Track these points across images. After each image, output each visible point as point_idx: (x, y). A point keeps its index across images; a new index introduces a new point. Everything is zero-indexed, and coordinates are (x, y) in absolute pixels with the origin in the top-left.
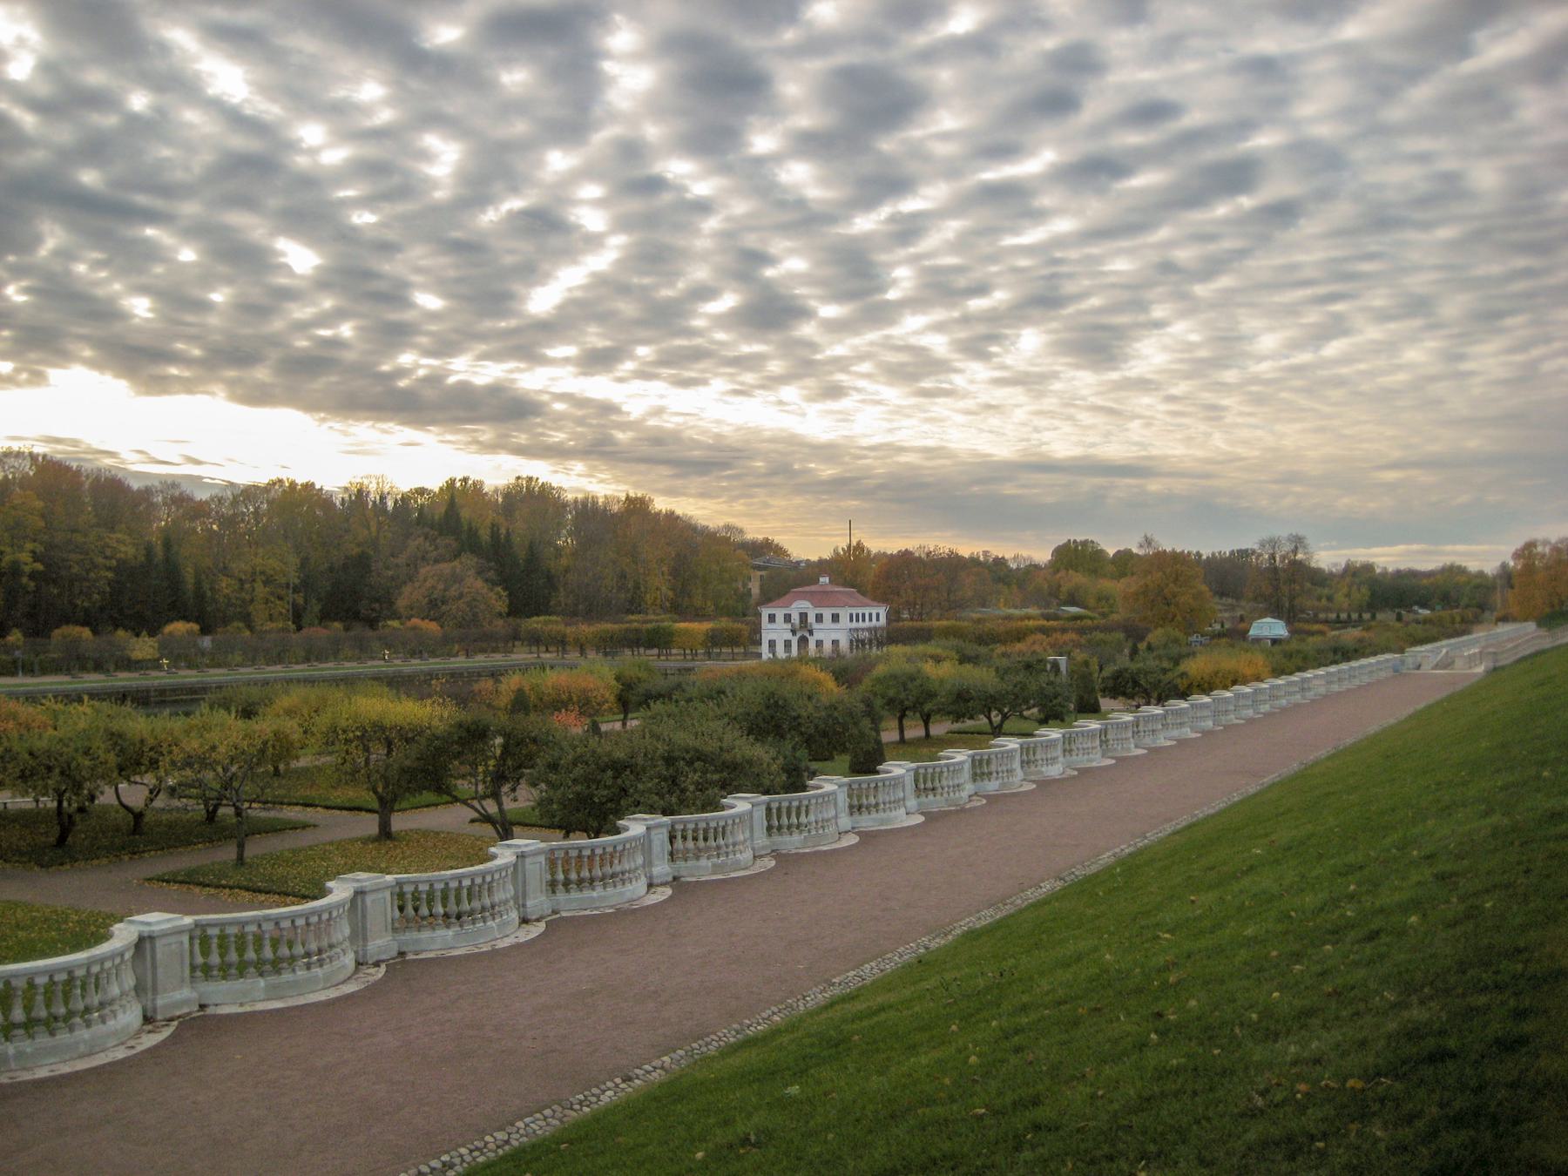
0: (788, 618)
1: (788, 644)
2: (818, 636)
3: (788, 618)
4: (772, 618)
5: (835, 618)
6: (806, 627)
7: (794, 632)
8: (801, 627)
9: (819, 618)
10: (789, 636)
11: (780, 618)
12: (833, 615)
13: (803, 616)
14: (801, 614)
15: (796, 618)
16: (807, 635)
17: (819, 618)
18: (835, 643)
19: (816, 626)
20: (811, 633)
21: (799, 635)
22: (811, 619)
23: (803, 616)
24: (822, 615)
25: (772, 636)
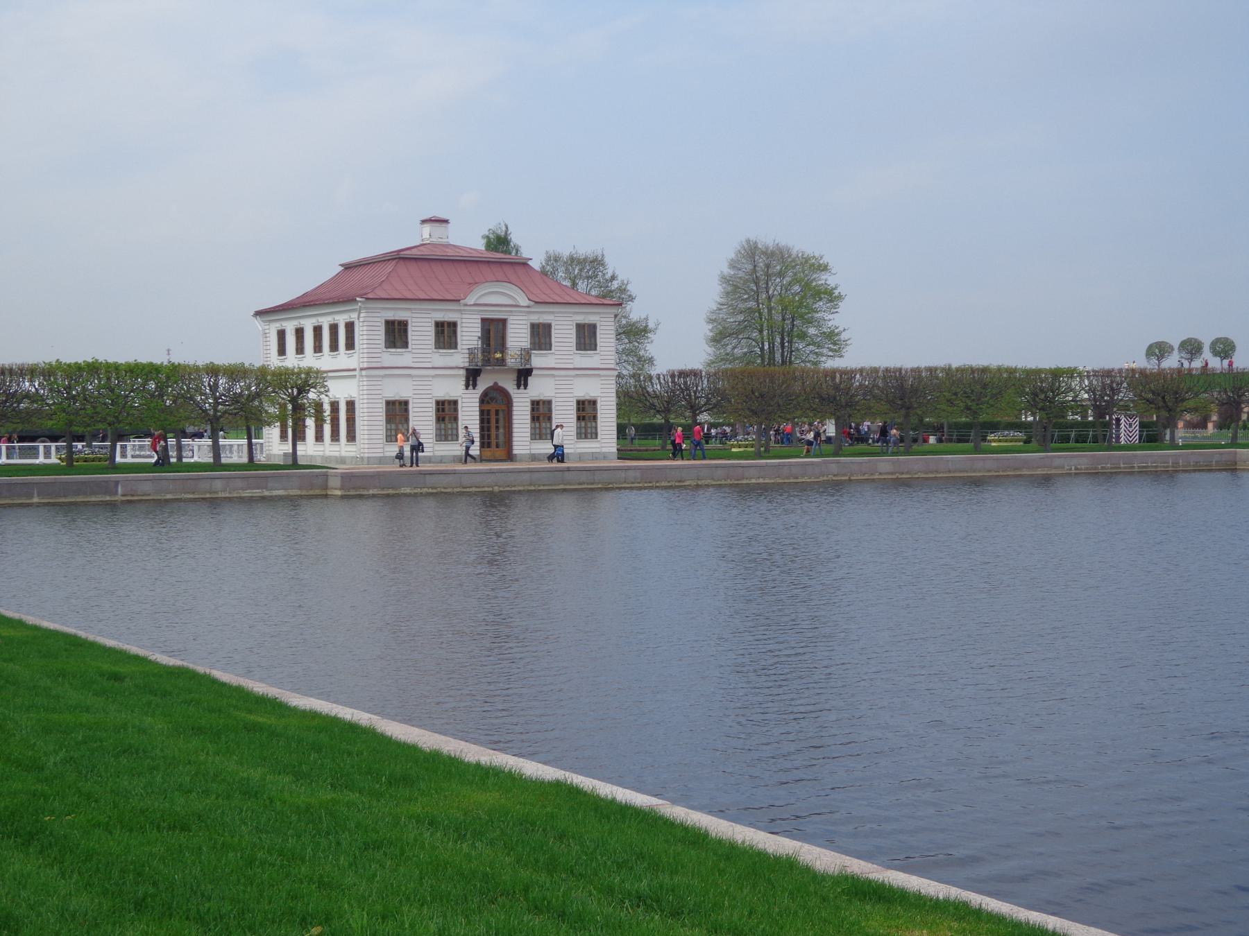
1: (446, 411)
2: (539, 388)
3: (446, 334)
4: (396, 334)
6: (502, 362)
7: (472, 376)
8: (487, 361)
9: (541, 336)
10: (454, 388)
12: (580, 328)
13: (493, 331)
15: (470, 335)
16: (509, 385)
17: (541, 336)
18: (586, 411)
20: (523, 376)
21: (484, 384)
22: (518, 337)
23: (493, 331)
24: (547, 328)
25: (398, 389)
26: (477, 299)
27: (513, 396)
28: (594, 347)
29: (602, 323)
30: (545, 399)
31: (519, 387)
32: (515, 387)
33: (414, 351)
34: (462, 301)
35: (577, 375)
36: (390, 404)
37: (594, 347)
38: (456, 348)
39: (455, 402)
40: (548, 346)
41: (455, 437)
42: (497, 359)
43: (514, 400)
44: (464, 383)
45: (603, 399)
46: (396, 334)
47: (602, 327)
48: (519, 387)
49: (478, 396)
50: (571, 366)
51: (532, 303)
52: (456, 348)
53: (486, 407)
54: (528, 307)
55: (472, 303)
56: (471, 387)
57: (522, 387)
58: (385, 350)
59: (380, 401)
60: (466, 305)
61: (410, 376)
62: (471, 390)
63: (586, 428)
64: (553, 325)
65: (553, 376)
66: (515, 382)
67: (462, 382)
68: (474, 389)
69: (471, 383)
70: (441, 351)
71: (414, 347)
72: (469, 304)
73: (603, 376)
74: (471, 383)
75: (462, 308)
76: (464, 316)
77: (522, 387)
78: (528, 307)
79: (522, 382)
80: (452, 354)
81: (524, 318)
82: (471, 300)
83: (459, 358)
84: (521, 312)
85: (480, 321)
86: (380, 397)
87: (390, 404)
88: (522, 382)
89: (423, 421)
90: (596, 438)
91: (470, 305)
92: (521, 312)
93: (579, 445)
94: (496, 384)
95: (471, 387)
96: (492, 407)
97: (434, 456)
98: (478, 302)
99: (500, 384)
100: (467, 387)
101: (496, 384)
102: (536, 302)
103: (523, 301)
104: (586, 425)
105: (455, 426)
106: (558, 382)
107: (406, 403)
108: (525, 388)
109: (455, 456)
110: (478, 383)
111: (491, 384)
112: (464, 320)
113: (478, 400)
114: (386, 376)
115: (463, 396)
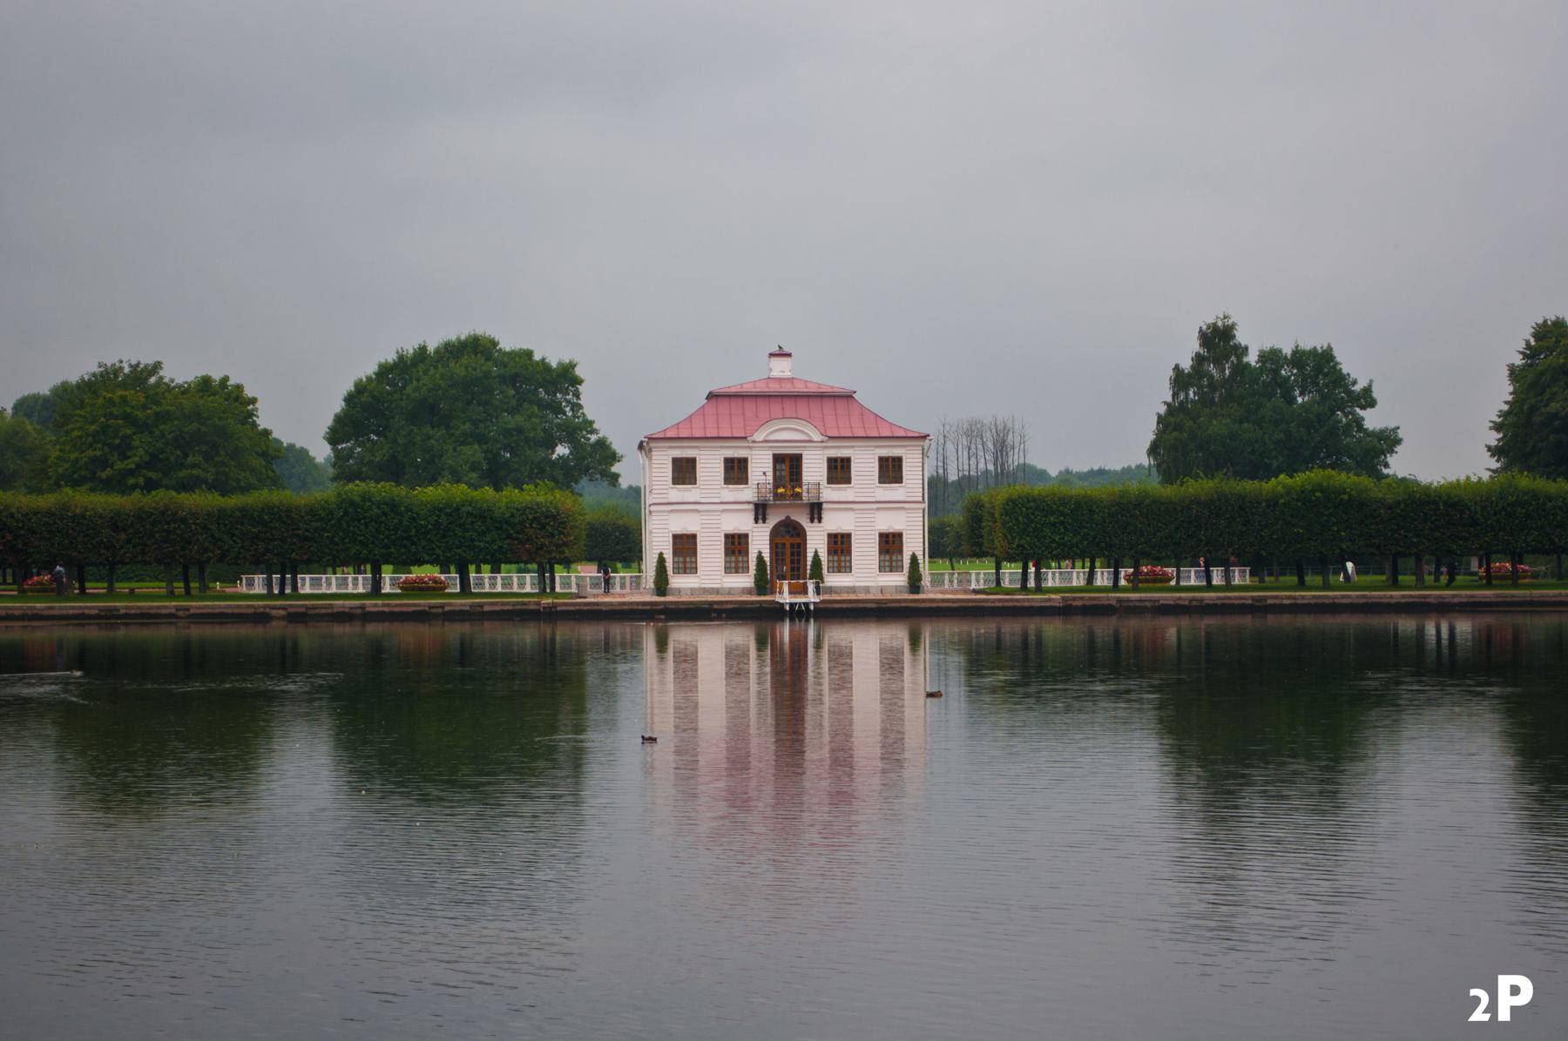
0: (736, 471)
1: (736, 545)
2: (834, 522)
3: (736, 471)
4: (684, 471)
5: (891, 470)
8: (776, 495)
9: (839, 470)
10: (742, 522)
11: (710, 464)
13: (789, 466)
14: (778, 459)
15: (761, 469)
16: (803, 520)
17: (839, 470)
18: (890, 544)
19: (830, 493)
20: (816, 511)
22: (814, 470)
23: (789, 466)
26: (767, 435)
27: (807, 529)
28: (898, 479)
29: (908, 456)
30: (843, 532)
31: (812, 521)
32: (809, 520)
33: (702, 487)
34: (749, 439)
35: (878, 509)
36: (677, 538)
37: (898, 479)
38: (747, 483)
39: (746, 536)
40: (847, 480)
41: (746, 569)
42: (782, 494)
43: (808, 533)
44: (753, 517)
45: (909, 532)
46: (684, 471)
47: (908, 460)
48: (812, 521)
49: (769, 530)
50: (873, 500)
51: (827, 438)
52: (747, 483)
53: (779, 541)
54: (822, 442)
55: (761, 439)
56: (760, 521)
57: (816, 520)
58: (672, 486)
59: (667, 535)
60: (754, 442)
61: (697, 511)
62: (760, 524)
63: (891, 561)
64: (852, 459)
65: (852, 509)
66: (809, 516)
67: (751, 516)
68: (764, 522)
69: (760, 517)
70: (730, 486)
71: (702, 483)
72: (757, 440)
73: (909, 509)
74: (760, 517)
75: (751, 445)
76: (754, 452)
77: (816, 520)
78: (822, 442)
79: (816, 516)
80: (742, 490)
81: (819, 452)
82: (759, 436)
83: (747, 493)
84: (817, 447)
85: (771, 457)
86: (667, 531)
87: (677, 538)
88: (816, 516)
89: (711, 555)
90: (851, 572)
91: (759, 442)
92: (817, 447)
93: (881, 579)
94: (788, 518)
95: (760, 521)
96: (788, 540)
97: (722, 588)
98: (768, 439)
99: (793, 518)
100: (756, 521)
101: (788, 518)
102: (830, 437)
103: (816, 436)
104: (891, 558)
105: (900, 558)
106: (857, 516)
107: (694, 537)
108: (820, 521)
109: (744, 588)
110: (767, 517)
111: (784, 518)
112: (754, 457)
113: (768, 534)
114: (672, 511)
115: (755, 530)
